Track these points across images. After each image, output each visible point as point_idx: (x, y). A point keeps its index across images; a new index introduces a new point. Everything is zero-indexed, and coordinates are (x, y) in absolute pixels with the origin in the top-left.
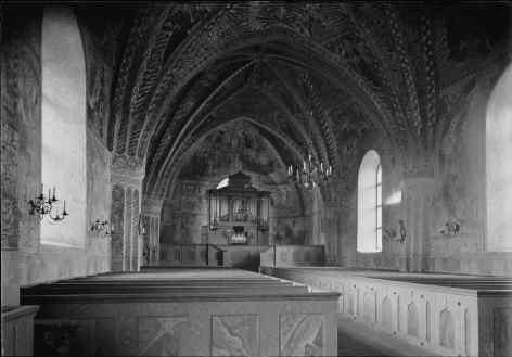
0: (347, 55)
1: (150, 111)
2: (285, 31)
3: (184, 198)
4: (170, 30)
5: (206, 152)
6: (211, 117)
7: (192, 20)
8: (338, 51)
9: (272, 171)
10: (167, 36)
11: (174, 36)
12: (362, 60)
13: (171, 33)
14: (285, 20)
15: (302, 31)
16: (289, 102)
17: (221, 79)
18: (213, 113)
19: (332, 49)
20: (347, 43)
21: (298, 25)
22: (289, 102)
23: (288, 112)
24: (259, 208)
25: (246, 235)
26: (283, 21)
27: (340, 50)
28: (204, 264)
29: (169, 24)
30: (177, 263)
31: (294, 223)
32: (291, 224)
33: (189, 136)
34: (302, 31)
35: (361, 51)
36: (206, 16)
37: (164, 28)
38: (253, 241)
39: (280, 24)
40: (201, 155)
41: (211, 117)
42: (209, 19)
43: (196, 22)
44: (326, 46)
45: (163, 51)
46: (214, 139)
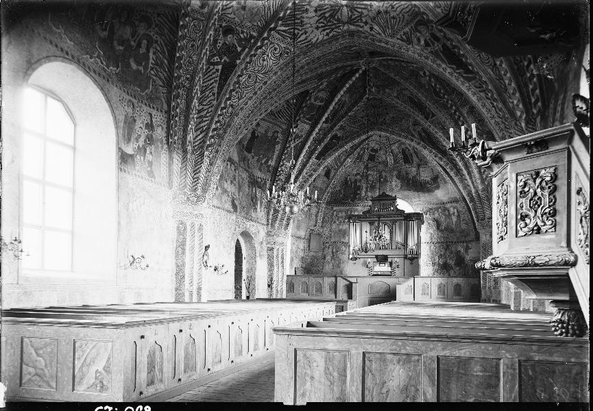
0: (427, 44)
1: (209, 146)
2: (352, 34)
3: (334, 226)
4: (218, 64)
5: (358, 174)
6: (335, 137)
7: (239, 49)
8: (415, 40)
9: (438, 187)
10: (217, 70)
12: (444, 46)
13: (220, 67)
15: (372, 29)
16: (420, 107)
17: (333, 95)
18: (336, 131)
19: (409, 41)
20: (421, 28)
21: (366, 23)
22: (420, 107)
23: (420, 118)
24: (391, 233)
25: (391, 264)
26: (348, 23)
27: (419, 40)
28: (333, 297)
29: (216, 59)
30: (305, 296)
31: (467, 249)
32: (462, 251)
33: (313, 160)
34: (372, 29)
36: (252, 41)
37: (209, 63)
38: (398, 272)
40: (353, 179)
41: (335, 137)
42: (255, 43)
43: (243, 50)
45: (216, 85)
46: (366, 157)
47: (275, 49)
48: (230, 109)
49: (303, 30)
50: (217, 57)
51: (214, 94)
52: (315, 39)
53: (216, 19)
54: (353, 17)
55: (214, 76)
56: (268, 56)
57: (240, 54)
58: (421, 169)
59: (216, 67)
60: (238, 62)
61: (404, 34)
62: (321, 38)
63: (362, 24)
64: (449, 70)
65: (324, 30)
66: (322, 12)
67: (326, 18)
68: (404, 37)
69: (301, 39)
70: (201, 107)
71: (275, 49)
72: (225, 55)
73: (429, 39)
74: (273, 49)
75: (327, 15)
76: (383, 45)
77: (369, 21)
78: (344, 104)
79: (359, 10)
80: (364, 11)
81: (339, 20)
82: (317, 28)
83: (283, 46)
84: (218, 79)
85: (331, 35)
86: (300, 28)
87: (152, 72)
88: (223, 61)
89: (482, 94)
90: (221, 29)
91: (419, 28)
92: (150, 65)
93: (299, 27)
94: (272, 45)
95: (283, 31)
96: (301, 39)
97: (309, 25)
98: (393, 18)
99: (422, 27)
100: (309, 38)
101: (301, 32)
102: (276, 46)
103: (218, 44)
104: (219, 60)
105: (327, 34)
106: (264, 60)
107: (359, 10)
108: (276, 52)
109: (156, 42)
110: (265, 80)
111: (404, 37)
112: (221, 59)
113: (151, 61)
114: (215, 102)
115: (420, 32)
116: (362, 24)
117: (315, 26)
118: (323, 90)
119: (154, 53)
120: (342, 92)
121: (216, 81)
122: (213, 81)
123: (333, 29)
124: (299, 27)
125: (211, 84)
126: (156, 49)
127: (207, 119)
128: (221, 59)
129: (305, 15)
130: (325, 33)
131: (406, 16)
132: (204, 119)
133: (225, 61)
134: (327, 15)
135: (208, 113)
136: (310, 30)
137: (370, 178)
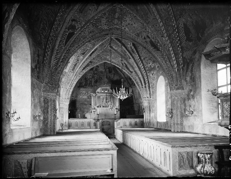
4: (67, 32)
7: (77, 28)
8: (141, 36)
10: (66, 35)
11: (69, 34)
13: (67, 34)
15: (125, 29)
21: (123, 26)
27: (142, 36)
35: (150, 36)
37: (65, 32)
39: (115, 26)
44: (136, 35)
46: (94, 69)
47: (89, 30)
52: (104, 28)
54: (119, 23)
55: (64, 36)
56: (86, 32)
58: (115, 76)
60: (75, 33)
61: (137, 33)
62: (106, 28)
64: (151, 48)
65: (108, 26)
67: (109, 21)
69: (99, 27)
75: (110, 21)
81: (113, 23)
82: (105, 25)
84: (66, 38)
85: (110, 28)
86: (100, 23)
87: (41, 32)
89: (162, 58)
92: (41, 29)
94: (88, 28)
96: (99, 27)
97: (103, 23)
98: (134, 27)
102: (90, 29)
105: (108, 27)
106: (84, 33)
109: (45, 20)
110: (84, 41)
112: (69, 30)
113: (41, 27)
114: (64, 48)
117: (105, 23)
119: (43, 24)
120: (98, 45)
121: (65, 39)
122: (63, 39)
123: (110, 26)
125: (63, 40)
126: (44, 22)
128: (69, 30)
129: (102, 19)
130: (108, 27)
131: (139, 27)
132: (58, 54)
134: (110, 21)
135: (60, 51)
136: (102, 25)
137: (95, 77)
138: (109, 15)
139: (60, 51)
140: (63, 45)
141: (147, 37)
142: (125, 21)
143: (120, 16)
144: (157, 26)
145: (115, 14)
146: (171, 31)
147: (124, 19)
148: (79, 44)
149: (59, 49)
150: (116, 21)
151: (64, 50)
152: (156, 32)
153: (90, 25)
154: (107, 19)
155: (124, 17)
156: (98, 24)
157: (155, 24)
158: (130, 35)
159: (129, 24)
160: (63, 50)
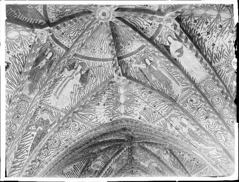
4: (34, 131)
7: (51, 123)
10: (33, 135)
13: (35, 133)
14: (126, 113)
21: (136, 115)
29: (33, 128)
47: (76, 125)
48: (38, 163)
49: (95, 116)
50: (34, 126)
51: (27, 151)
53: (38, 102)
57: (51, 125)
59: (33, 133)
60: (49, 130)
63: (133, 115)
65: (109, 117)
66: (109, 106)
68: (162, 124)
70: (16, 160)
71: (76, 125)
72: (40, 126)
73: (179, 126)
74: (74, 125)
75: (111, 108)
76: (148, 127)
77: (138, 114)
78: (112, 170)
79: (131, 107)
80: (135, 108)
81: (119, 112)
82: (104, 115)
83: (81, 124)
86: (93, 114)
88: (38, 129)
90: (40, 109)
91: (172, 119)
93: (92, 114)
95: (82, 115)
99: (174, 118)
100: (98, 121)
101: (94, 117)
102: (76, 124)
103: (37, 118)
104: (35, 128)
105: (111, 120)
107: (131, 107)
108: (76, 127)
110: (67, 145)
111: (162, 124)
114: (27, 157)
115: (172, 121)
116: (133, 115)
117: (103, 114)
118: (100, 160)
121: (30, 143)
122: (28, 142)
124: (92, 114)
127: (19, 168)
129: (97, 107)
130: (109, 119)
133: (40, 130)
135: (21, 164)
136: (99, 116)
138: (108, 99)
139: (21, 164)
140: (26, 153)
141: (181, 126)
142: (138, 106)
143: (128, 98)
144: (192, 101)
145: (119, 97)
146: (221, 104)
147: (136, 103)
148: (59, 151)
149: (20, 160)
150: (122, 109)
151: (28, 161)
152: (194, 112)
153: (73, 115)
154: (106, 107)
155: (135, 99)
156: (91, 116)
157: (189, 99)
158: (150, 126)
159: (145, 109)
160: (25, 161)
